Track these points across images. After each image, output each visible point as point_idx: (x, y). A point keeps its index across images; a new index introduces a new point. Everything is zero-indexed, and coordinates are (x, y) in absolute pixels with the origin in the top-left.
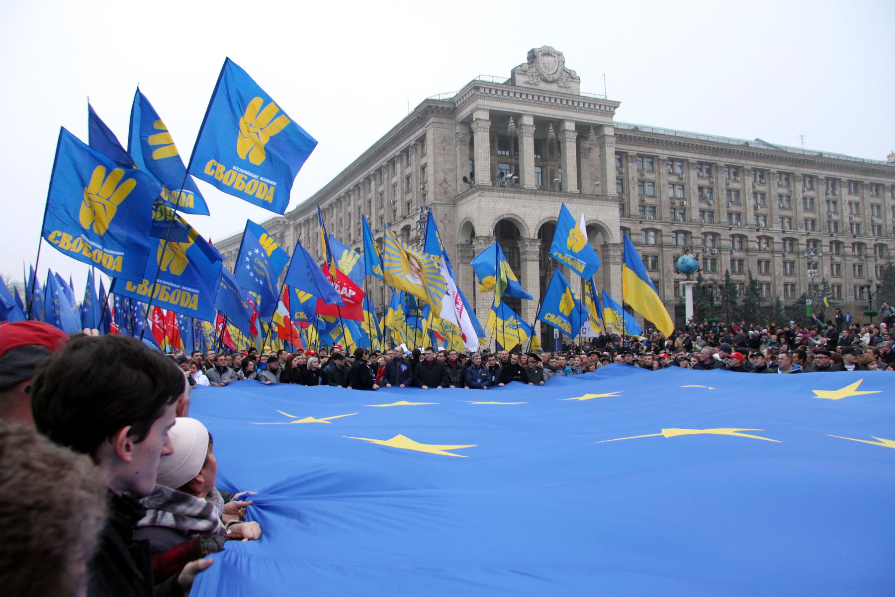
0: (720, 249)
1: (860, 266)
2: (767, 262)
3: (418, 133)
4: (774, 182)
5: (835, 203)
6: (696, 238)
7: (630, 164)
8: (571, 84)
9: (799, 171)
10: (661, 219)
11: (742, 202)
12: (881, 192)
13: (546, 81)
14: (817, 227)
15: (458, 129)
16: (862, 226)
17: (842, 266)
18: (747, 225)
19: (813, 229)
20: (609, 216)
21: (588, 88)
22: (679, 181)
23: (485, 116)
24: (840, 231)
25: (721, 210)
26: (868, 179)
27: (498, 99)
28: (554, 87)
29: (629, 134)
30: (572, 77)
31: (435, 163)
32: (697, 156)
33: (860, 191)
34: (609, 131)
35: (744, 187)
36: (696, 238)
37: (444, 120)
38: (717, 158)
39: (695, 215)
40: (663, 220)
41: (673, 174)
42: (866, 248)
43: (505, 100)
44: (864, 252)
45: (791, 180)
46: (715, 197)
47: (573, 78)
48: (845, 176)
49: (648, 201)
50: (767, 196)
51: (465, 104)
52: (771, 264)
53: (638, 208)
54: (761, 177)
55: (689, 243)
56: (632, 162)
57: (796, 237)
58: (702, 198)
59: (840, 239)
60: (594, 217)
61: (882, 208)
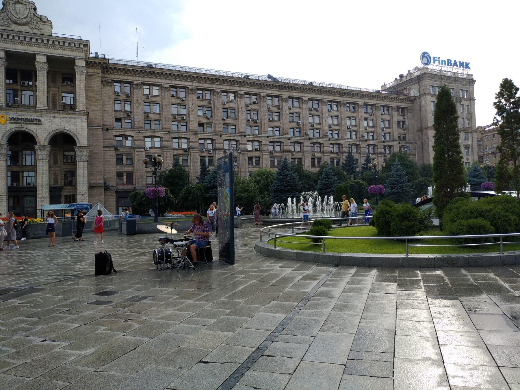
6: (193, 142)
7: (135, 91)
8: (42, 26)
11: (237, 117)
13: (16, 23)
20: (77, 127)
21: (59, 30)
22: (182, 102)
25: (217, 122)
28: (25, 29)
29: (131, 68)
30: (45, 21)
34: (80, 63)
35: (238, 107)
36: (193, 142)
38: (214, 86)
40: (164, 130)
41: (177, 97)
42: (342, 147)
47: (44, 22)
49: (152, 116)
53: (143, 121)
56: (137, 89)
60: (62, 127)
61: (357, 119)
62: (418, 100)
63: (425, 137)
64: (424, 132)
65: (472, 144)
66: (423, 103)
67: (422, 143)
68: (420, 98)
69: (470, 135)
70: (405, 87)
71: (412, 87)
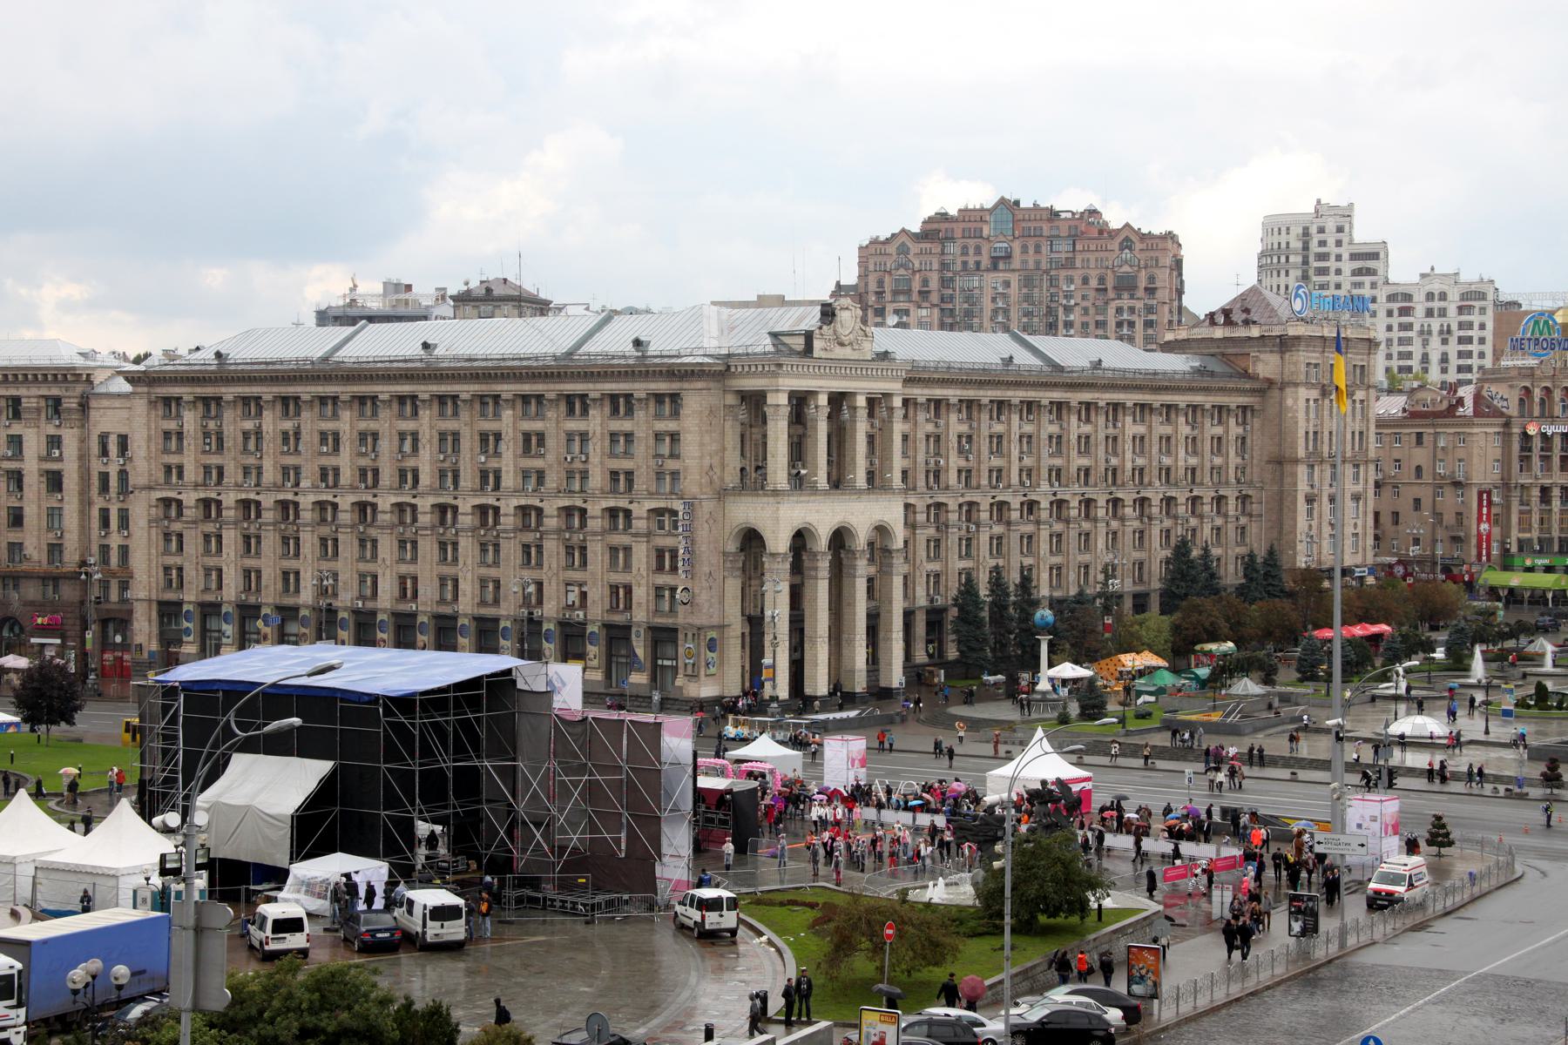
0: (978, 525)
1: (1141, 532)
2: (1030, 537)
3: (662, 386)
4: (1045, 418)
5: (1115, 439)
9: (1076, 397)
10: (914, 489)
11: (1005, 451)
12: (1173, 416)
13: (842, 344)
14: (1092, 480)
15: (731, 399)
16: (1146, 471)
17: (1120, 534)
18: (1009, 486)
19: (1086, 484)
23: (783, 399)
24: (1119, 482)
26: (1157, 400)
27: (798, 376)
31: (702, 445)
32: (959, 392)
33: (1147, 417)
35: (1009, 431)
37: (712, 385)
39: (952, 478)
43: (803, 376)
44: (1147, 511)
45: (1064, 412)
46: (975, 448)
48: (1129, 398)
50: (1034, 439)
51: (749, 375)
52: (1035, 539)
54: (1029, 412)
55: (942, 519)
57: (1066, 497)
58: (961, 451)
59: (1120, 495)
61: (1173, 441)
62: (1276, 393)
63: (1288, 480)
64: (1288, 468)
65: (1365, 490)
66: (1289, 402)
67: (1282, 492)
68: (1281, 389)
69: (1362, 468)
70: (1246, 350)
71: (1262, 356)
